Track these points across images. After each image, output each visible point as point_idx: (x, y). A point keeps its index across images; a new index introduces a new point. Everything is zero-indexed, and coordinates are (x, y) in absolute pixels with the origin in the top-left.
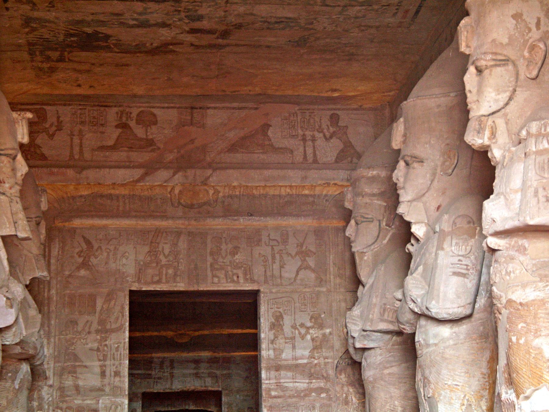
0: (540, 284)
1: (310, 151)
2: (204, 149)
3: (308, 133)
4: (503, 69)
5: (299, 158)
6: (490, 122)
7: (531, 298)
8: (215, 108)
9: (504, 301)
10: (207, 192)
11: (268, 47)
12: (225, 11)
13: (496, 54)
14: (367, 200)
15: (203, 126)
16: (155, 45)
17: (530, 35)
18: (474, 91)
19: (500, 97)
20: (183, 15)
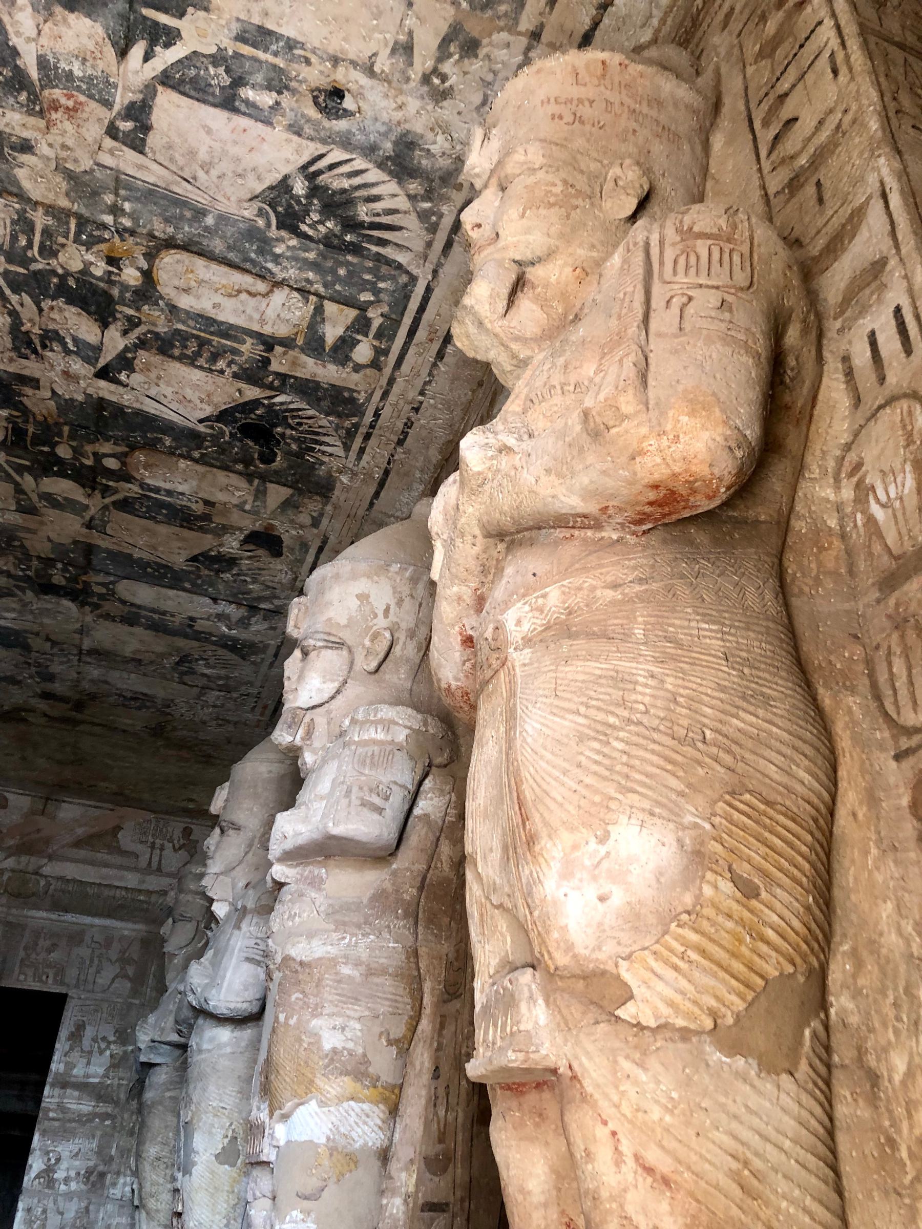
0: (334, 934)
1: (155, 859)
2: (47, 841)
3: (158, 841)
4: (335, 652)
5: (143, 863)
6: (307, 719)
7: (318, 955)
8: (70, 803)
9: (278, 959)
10: (38, 883)
11: (124, 731)
12: (79, 673)
13: (329, 634)
14: (189, 897)
15: (53, 818)
16: (6, 708)
17: (375, 621)
18: (294, 678)
19: (325, 686)
20: (33, 669)
